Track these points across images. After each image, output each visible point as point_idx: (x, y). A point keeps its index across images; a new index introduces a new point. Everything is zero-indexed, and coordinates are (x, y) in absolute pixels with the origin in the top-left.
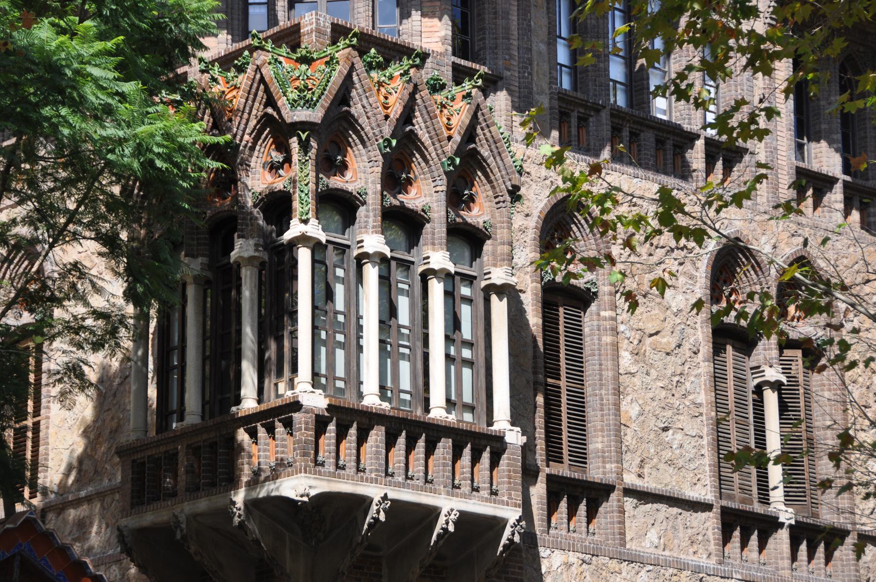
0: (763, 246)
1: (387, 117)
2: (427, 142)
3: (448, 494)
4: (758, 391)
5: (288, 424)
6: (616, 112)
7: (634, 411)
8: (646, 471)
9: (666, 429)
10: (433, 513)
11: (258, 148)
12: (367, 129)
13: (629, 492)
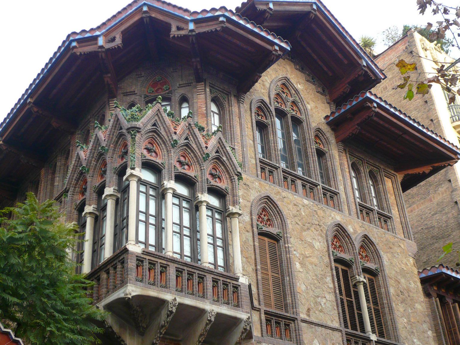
0: (350, 229)
1: (175, 133)
2: (196, 149)
3: (210, 303)
4: (355, 286)
5: (123, 262)
7: (303, 287)
8: (311, 313)
9: (318, 297)
11: (116, 150)
12: (166, 137)
13: (304, 321)
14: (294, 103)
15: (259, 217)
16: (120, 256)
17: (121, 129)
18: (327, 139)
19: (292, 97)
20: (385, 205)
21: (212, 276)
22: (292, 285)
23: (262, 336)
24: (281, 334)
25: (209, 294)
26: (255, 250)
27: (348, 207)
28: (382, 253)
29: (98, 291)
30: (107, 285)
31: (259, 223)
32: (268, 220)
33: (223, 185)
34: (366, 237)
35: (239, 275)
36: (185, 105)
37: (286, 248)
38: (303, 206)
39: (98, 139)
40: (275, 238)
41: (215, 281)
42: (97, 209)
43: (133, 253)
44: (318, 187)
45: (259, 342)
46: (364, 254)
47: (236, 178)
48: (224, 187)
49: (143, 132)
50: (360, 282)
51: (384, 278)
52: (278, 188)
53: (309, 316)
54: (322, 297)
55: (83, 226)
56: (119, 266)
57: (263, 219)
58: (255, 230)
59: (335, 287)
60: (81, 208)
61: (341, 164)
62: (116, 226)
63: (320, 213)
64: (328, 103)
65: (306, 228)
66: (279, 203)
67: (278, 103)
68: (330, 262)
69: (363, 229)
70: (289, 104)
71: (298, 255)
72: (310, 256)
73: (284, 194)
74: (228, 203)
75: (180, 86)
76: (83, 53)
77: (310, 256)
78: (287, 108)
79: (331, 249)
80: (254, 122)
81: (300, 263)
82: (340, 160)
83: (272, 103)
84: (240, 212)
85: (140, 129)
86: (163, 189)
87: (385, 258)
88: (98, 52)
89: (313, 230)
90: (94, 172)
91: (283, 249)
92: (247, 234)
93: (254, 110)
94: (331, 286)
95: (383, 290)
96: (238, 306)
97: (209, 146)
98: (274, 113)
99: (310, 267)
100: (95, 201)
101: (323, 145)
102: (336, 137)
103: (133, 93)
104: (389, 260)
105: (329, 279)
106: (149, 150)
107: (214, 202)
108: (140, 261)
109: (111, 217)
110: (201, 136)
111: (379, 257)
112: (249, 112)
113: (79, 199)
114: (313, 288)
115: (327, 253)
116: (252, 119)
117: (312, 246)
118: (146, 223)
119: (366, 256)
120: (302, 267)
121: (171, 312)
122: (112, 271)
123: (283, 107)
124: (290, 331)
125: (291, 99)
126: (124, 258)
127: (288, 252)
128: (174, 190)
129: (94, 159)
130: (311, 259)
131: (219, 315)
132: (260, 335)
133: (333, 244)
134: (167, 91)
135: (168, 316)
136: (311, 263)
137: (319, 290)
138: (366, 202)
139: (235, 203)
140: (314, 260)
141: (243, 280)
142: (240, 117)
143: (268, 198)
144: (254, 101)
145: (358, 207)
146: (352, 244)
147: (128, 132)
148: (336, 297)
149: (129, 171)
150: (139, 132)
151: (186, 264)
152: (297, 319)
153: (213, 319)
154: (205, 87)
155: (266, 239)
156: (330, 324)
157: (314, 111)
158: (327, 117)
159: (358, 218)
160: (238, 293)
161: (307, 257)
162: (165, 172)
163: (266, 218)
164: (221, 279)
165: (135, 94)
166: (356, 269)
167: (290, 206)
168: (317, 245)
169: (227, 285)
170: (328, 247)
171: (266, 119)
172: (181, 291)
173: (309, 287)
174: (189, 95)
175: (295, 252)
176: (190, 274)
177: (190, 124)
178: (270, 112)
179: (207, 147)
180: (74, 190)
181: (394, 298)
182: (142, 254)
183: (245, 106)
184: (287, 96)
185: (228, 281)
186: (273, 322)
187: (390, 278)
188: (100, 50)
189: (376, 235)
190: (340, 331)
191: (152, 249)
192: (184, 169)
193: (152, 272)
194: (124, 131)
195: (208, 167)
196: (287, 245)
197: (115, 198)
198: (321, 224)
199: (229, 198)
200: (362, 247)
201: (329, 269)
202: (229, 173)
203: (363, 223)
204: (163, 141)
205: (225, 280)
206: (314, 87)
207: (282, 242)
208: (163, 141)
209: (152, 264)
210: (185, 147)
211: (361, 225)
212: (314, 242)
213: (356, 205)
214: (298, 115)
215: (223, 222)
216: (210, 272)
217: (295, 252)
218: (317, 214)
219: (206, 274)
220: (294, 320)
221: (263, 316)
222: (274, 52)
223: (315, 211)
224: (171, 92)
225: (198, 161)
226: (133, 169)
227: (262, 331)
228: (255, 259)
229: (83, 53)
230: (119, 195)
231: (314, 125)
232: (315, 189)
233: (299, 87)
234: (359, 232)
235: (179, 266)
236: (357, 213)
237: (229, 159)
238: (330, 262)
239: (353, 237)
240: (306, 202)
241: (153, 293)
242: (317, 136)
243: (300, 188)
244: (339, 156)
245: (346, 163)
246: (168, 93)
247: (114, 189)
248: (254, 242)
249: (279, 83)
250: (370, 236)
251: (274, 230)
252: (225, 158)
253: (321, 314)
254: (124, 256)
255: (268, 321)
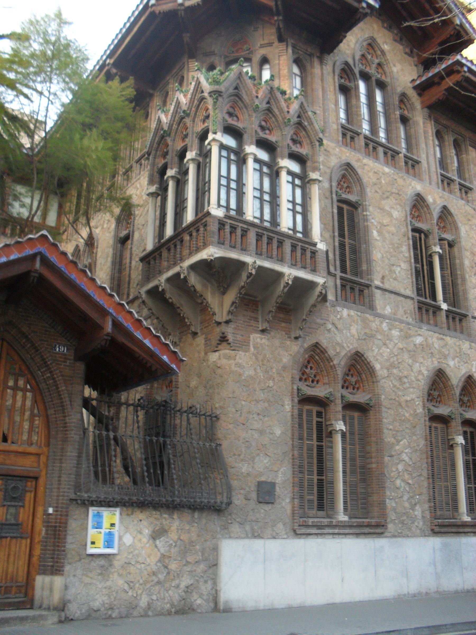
0: (430, 199)
1: (257, 97)
2: (278, 113)
3: (289, 267)
4: (431, 256)
6: (366, 137)
8: (385, 280)
9: (393, 265)
10: (280, 275)
13: (378, 288)
14: (379, 65)
15: (339, 184)
16: (203, 219)
17: (202, 92)
18: (412, 105)
19: (377, 58)
20: (467, 176)
21: (291, 241)
22: (368, 253)
23: (337, 300)
24: (355, 299)
25: (287, 258)
26: (333, 217)
27: (430, 176)
28: (460, 225)
29: (181, 252)
30: (190, 247)
31: (338, 190)
32: (348, 187)
33: (304, 151)
34: (445, 208)
35: (316, 241)
36: (267, 66)
37: (364, 215)
38: (384, 174)
39: (179, 103)
40: (354, 206)
41: (294, 247)
42: (179, 173)
43: (215, 217)
44: (400, 155)
45: (333, 306)
46: (442, 225)
47: (317, 144)
48: (304, 153)
49: (225, 96)
50: (435, 252)
51: (460, 249)
52: (359, 156)
53: (383, 283)
54: (397, 266)
55: (166, 189)
56: (202, 229)
57: (342, 186)
58: (334, 196)
59: (410, 256)
60: (163, 171)
61: (425, 132)
62: (198, 190)
63: (400, 181)
64: (416, 66)
65: (385, 196)
66: (359, 171)
67: (362, 64)
68: (408, 231)
69: (443, 200)
70: (374, 66)
71: (375, 224)
72: (388, 225)
73: (366, 161)
74: (308, 169)
75: (262, 46)
76: (162, 11)
77: (388, 225)
78: (372, 70)
79: (409, 219)
80: (337, 85)
81: (377, 231)
82: (424, 127)
83: (357, 65)
84: (320, 179)
85: (221, 92)
86: (244, 153)
87: (463, 230)
88: (178, 10)
89: (392, 198)
90: (175, 135)
91: (361, 217)
92: (326, 201)
93: (337, 71)
94: (407, 255)
95: (457, 261)
96: (314, 271)
97: (291, 111)
98: (358, 76)
99: (387, 235)
100: (177, 165)
101: (408, 111)
102: (422, 103)
103: (212, 54)
104: (466, 232)
105: (404, 248)
106: (230, 114)
107: (295, 167)
108: (222, 224)
109: (193, 181)
110: (282, 101)
111: (457, 228)
112: (332, 75)
113: (160, 162)
114: (389, 257)
115: (405, 223)
116: (334, 82)
117: (390, 215)
118: (228, 188)
119: (444, 227)
120: (379, 235)
121: (251, 274)
122: (194, 234)
123: (368, 70)
124: (364, 296)
125: (377, 61)
126: (206, 221)
127: (366, 220)
128: (255, 155)
129: (175, 123)
130: (388, 228)
131: (296, 279)
132: (334, 299)
133: (411, 214)
134: (247, 52)
135: (248, 277)
136: (389, 232)
137: (393, 258)
138: (447, 172)
139: (315, 169)
140: (392, 229)
141: (321, 246)
142: (322, 80)
143: (349, 165)
144: (338, 63)
145: (439, 176)
146: (431, 214)
147: (211, 96)
148: (411, 266)
149: (211, 136)
150: (220, 96)
151: (265, 229)
152: (371, 285)
153: (290, 282)
154: (287, 47)
155: (345, 207)
156: (402, 291)
157: (400, 74)
158: (413, 81)
159: (438, 188)
160: (315, 259)
161: (385, 226)
162: (245, 137)
163: (345, 185)
164: (300, 244)
165: (215, 54)
166: (433, 239)
167: (371, 174)
168: (396, 214)
169: (305, 250)
170: (406, 216)
171: (350, 82)
172: (261, 255)
173: (385, 255)
174: (270, 57)
175: (373, 221)
176: (270, 239)
177: (272, 88)
178: (354, 74)
179: (288, 112)
180: (156, 153)
181: (468, 270)
182: (224, 218)
183: (328, 68)
184: (372, 57)
185: (307, 246)
186: (348, 288)
187: (466, 250)
188: (179, 8)
189: (455, 207)
190: (412, 299)
191: (233, 213)
192: (265, 134)
193: (233, 235)
194: (206, 94)
195: (289, 132)
196: (365, 213)
197: (196, 162)
198: (400, 193)
199: (309, 164)
200: (440, 218)
201: (406, 238)
202: (310, 139)
203: (443, 194)
204: (244, 105)
205: (303, 245)
206: (401, 47)
207: (360, 210)
208: (244, 105)
209: (233, 228)
210: (266, 112)
211: (441, 195)
212: (392, 211)
213: (437, 174)
214: (383, 78)
215: (303, 187)
216: (289, 237)
217: (373, 221)
218: (397, 183)
219: (285, 239)
220: (368, 286)
221: (339, 282)
222: (361, 10)
223: (396, 180)
224: (251, 52)
225: (279, 126)
226: (215, 133)
227: (336, 295)
228: (333, 226)
229: (162, 11)
230: (201, 160)
231: (399, 90)
232: (397, 157)
233: (386, 47)
234: (439, 202)
235: (260, 231)
236: (438, 183)
237: (311, 124)
238: (408, 231)
239: (432, 207)
240: (387, 170)
241: (234, 255)
242: (401, 101)
243: (381, 155)
244: (424, 123)
245: (430, 131)
246: (249, 54)
247: (196, 153)
248: (332, 208)
249: (365, 44)
250: (449, 207)
251: (352, 198)
252: (306, 124)
253: (395, 282)
254: (208, 219)
255: (343, 286)
